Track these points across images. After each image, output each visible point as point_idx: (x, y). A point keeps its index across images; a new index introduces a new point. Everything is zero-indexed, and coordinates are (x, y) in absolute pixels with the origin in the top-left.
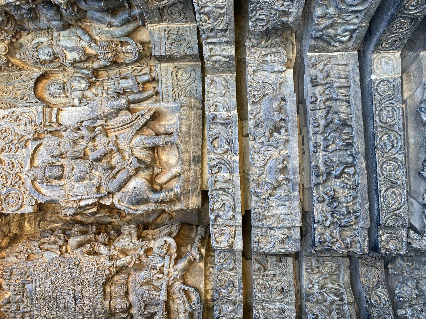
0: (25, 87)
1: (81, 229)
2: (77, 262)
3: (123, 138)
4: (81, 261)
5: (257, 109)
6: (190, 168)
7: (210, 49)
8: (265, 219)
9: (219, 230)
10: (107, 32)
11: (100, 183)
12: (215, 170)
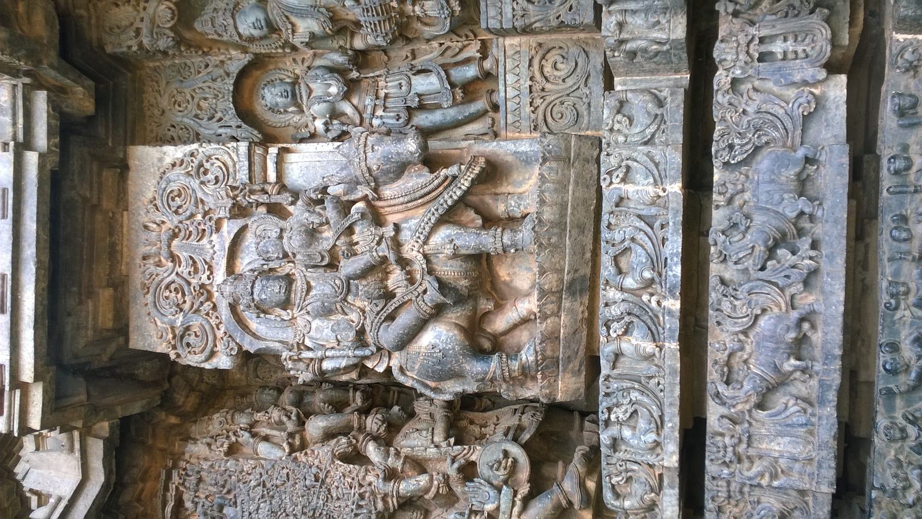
0: (216, 92)
1: (332, 396)
2: (321, 475)
3: (410, 229)
4: (329, 475)
5: (738, 180)
6: (559, 308)
7: (621, 25)
8: (740, 461)
9: (622, 468)
11: (363, 324)
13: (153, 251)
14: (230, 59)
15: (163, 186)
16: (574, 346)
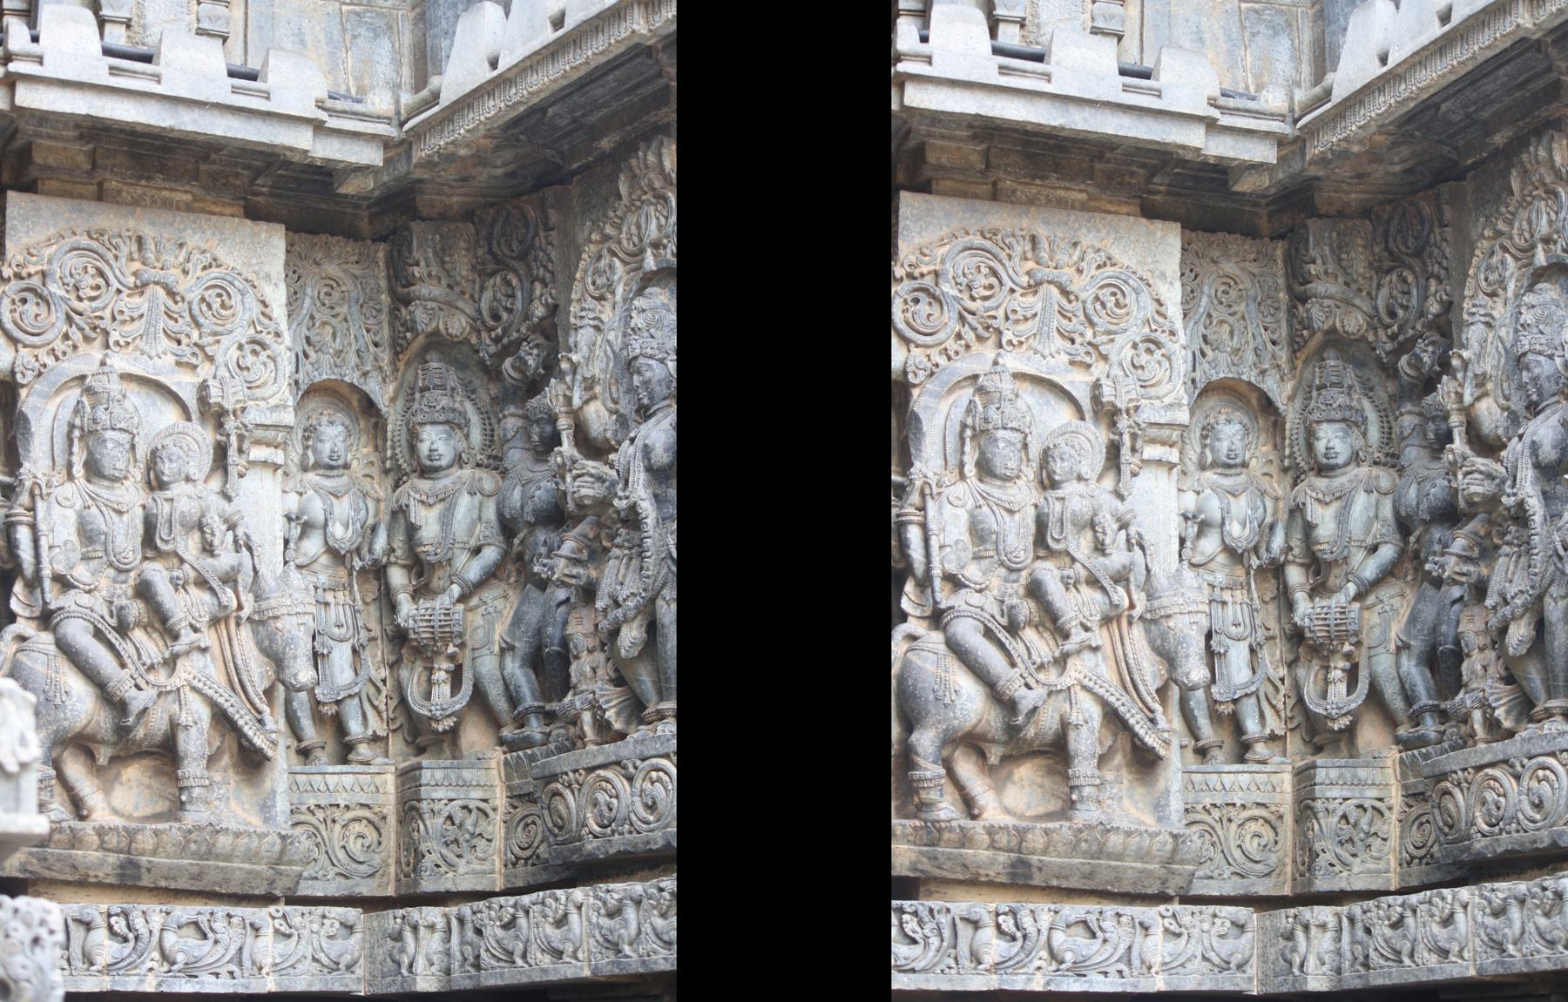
10: (1386, 630)
11: (966, 586)
12: (1008, 924)
13: (1043, 254)
14: (1282, 379)
15: (1131, 281)
16: (948, 864)
